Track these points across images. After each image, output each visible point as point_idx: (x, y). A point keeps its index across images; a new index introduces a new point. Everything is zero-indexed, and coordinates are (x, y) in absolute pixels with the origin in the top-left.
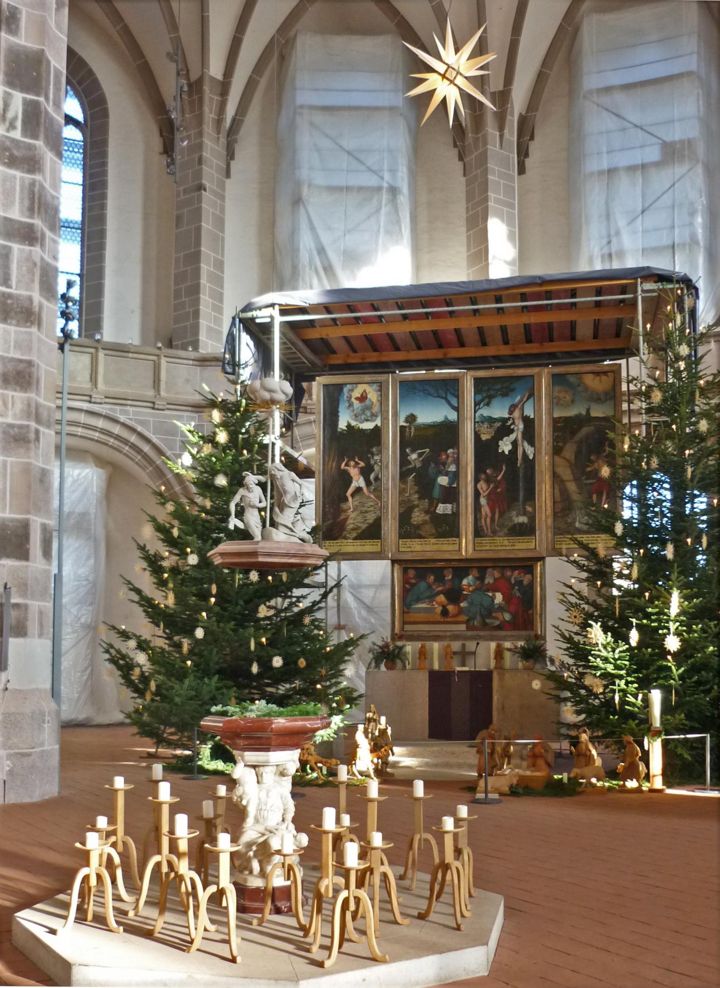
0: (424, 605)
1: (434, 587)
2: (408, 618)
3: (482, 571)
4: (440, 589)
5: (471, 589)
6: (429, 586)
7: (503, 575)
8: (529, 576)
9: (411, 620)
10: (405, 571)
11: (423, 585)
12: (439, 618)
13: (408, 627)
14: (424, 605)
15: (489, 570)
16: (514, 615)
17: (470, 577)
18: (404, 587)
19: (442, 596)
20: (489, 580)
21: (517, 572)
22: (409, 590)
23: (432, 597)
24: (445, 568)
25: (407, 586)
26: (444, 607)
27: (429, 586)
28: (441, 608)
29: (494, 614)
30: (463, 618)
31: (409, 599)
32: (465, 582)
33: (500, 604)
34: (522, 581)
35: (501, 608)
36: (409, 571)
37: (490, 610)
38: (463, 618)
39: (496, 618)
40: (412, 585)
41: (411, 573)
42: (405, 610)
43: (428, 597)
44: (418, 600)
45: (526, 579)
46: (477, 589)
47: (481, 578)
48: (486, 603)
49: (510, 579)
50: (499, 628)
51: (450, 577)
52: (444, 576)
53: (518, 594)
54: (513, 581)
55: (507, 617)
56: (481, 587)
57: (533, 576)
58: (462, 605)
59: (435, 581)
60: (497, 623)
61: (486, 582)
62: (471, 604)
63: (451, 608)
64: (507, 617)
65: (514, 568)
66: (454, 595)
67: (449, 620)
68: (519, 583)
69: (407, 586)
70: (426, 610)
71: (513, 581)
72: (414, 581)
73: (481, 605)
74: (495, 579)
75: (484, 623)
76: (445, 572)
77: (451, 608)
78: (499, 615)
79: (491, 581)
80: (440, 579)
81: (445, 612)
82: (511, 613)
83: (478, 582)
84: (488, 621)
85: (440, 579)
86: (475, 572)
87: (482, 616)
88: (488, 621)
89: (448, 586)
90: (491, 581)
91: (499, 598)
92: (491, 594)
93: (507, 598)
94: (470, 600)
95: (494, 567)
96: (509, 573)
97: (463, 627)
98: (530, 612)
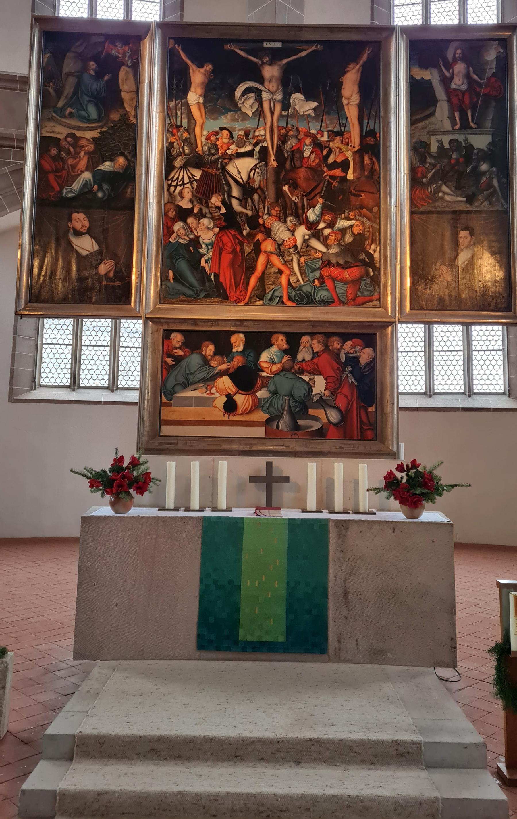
0: (196, 394)
1: (213, 364)
2: (167, 414)
3: (294, 340)
4: (224, 367)
5: (275, 368)
6: (206, 362)
7: (326, 347)
8: (369, 351)
9: (173, 417)
10: (167, 334)
11: (195, 360)
12: (219, 415)
13: (167, 430)
14: (196, 394)
15: (305, 339)
16: (345, 415)
17: (274, 349)
18: (164, 362)
19: (226, 379)
20: (304, 355)
21: (349, 343)
22: (173, 366)
23: (210, 380)
24: (234, 333)
25: (169, 361)
26: (229, 397)
27: (206, 362)
28: (224, 399)
29: (311, 412)
30: (261, 416)
31: (171, 383)
32: (265, 356)
33: (321, 395)
34: (357, 359)
35: (322, 403)
36: (173, 335)
37: (303, 406)
38: (261, 416)
39: (316, 418)
40: (178, 360)
41: (177, 339)
42: (164, 400)
43: (202, 381)
44: (186, 385)
45: (365, 355)
46: (283, 369)
47: (292, 350)
48: (300, 392)
49: (338, 355)
50: (320, 434)
51: (241, 348)
52: (231, 347)
53: (351, 379)
54: (343, 359)
55: (334, 416)
56: (292, 369)
57: (375, 351)
58: (259, 394)
59: (216, 353)
60: (317, 426)
61: (300, 357)
62: (274, 393)
63: (240, 399)
64: (334, 416)
65: (345, 337)
66: (246, 378)
67: (237, 418)
68: (353, 361)
69: (169, 361)
70: (200, 402)
71: (343, 359)
72: (180, 353)
73: (291, 395)
74: (315, 355)
75: (295, 426)
76: (233, 339)
77: (240, 399)
78: (320, 413)
79: (308, 357)
80: (224, 349)
81: (230, 406)
82: (339, 410)
83: (286, 358)
84: (300, 422)
85: (224, 349)
86: (281, 341)
87: (291, 413)
88: (300, 422)
89: (238, 361)
90: (308, 357)
91: (320, 385)
92: (307, 379)
93: (334, 388)
94: (272, 388)
95: (312, 334)
96: (336, 344)
97: (260, 432)
98: (371, 409)
